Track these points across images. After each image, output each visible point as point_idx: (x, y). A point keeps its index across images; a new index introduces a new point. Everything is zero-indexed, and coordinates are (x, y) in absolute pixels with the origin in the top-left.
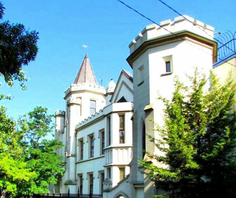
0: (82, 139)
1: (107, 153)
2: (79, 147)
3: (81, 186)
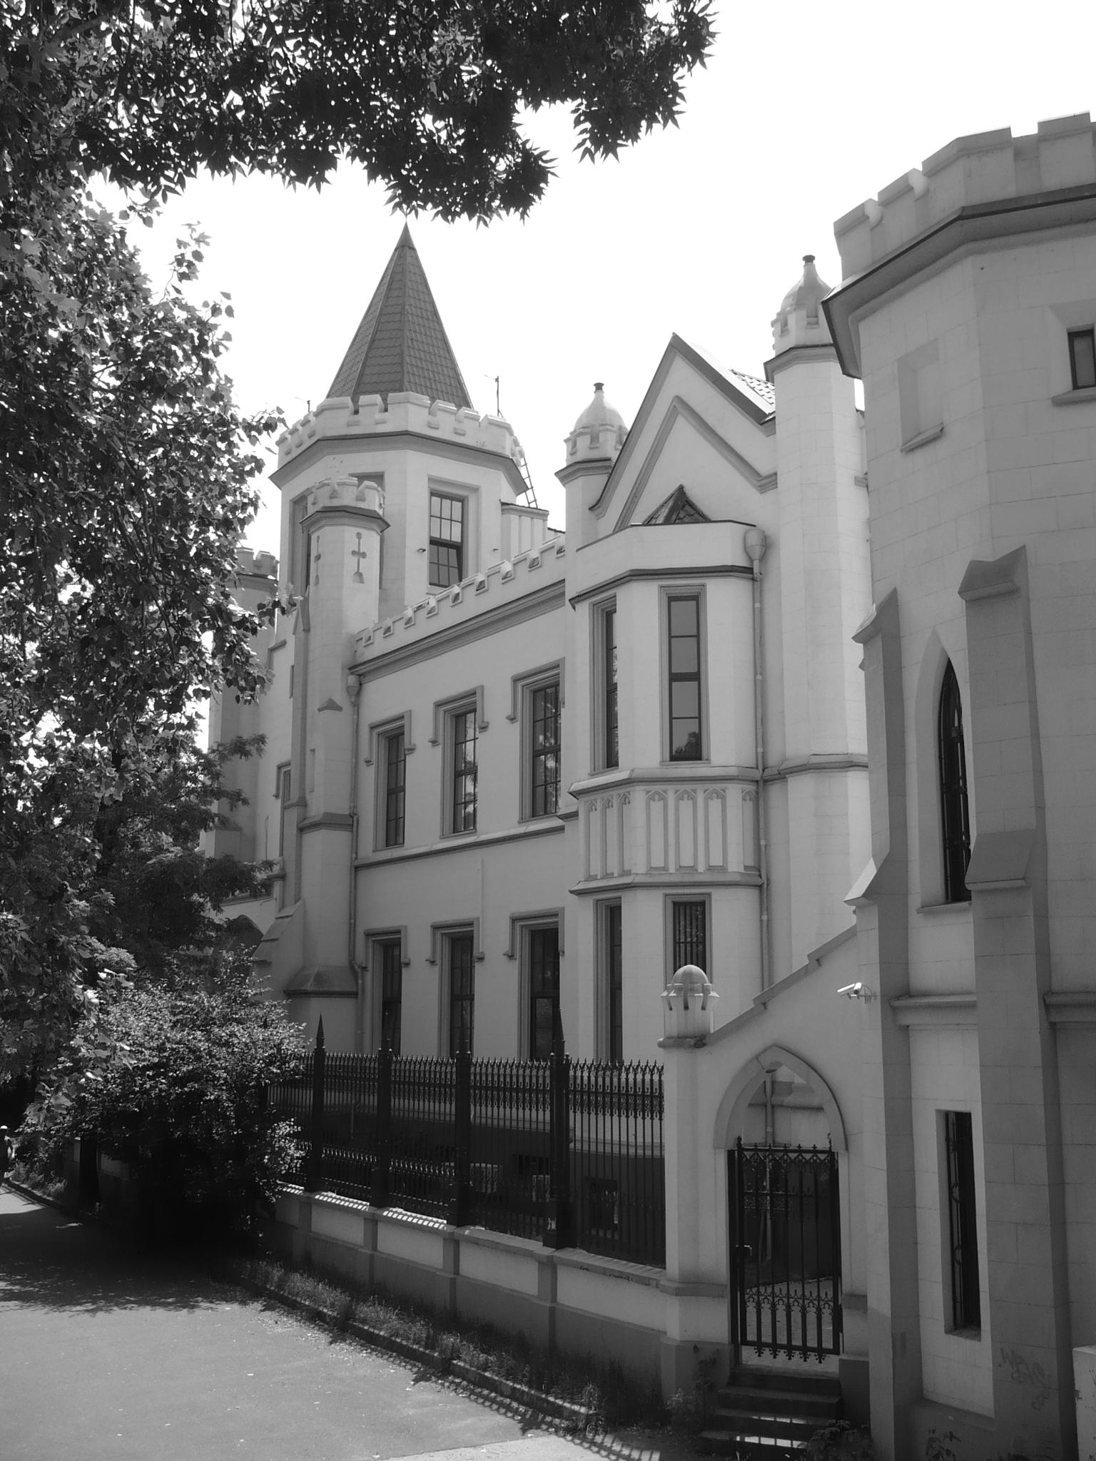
0: (399, 723)
1: (596, 817)
2: (372, 769)
3: (391, 1005)
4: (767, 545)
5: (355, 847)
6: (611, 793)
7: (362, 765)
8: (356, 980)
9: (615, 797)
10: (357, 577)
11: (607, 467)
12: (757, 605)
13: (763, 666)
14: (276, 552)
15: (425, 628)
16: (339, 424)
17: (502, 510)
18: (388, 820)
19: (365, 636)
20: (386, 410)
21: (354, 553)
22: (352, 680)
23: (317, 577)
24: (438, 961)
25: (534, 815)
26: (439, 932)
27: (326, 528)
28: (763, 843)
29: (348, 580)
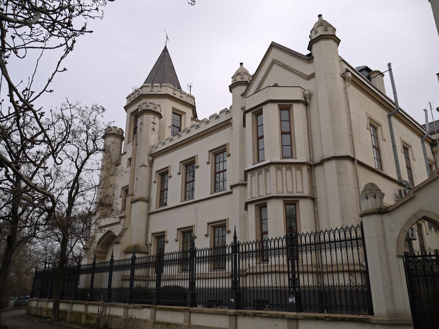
1: (255, 179)
2: (156, 184)
4: (310, 96)
5: (149, 207)
6: (261, 169)
9: (263, 170)
10: (153, 130)
17: (192, 120)
18: (160, 200)
19: (155, 146)
21: (152, 123)
22: (151, 158)
23: (141, 129)
24: (179, 240)
27: (145, 115)
28: (314, 185)
29: (151, 130)
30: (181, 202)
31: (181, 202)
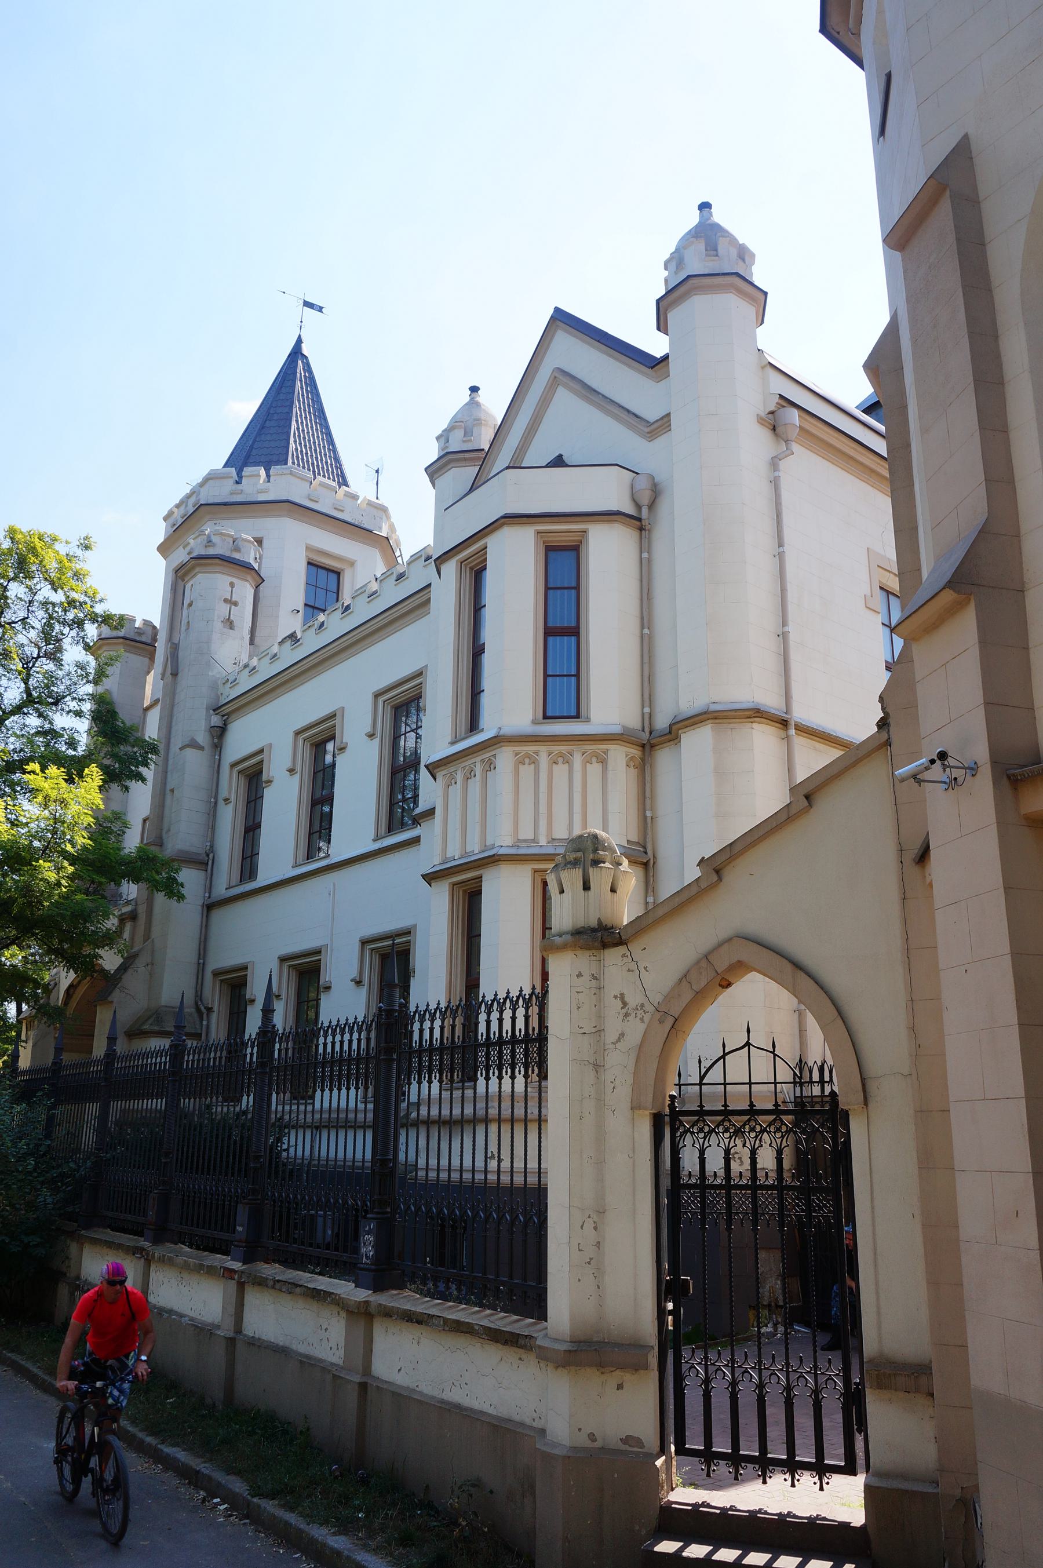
2: (231, 807)
5: (209, 887)
6: (473, 760)
7: (221, 802)
8: (201, 1020)
9: (478, 765)
11: (478, 459)
12: (645, 555)
13: (650, 621)
14: (157, 624)
15: (290, 656)
16: (223, 491)
18: (243, 859)
20: (269, 481)
21: (225, 601)
25: (391, 830)
26: (286, 965)
27: (199, 576)
28: (648, 814)
29: (218, 625)
30: (293, 867)
31: (293, 867)
